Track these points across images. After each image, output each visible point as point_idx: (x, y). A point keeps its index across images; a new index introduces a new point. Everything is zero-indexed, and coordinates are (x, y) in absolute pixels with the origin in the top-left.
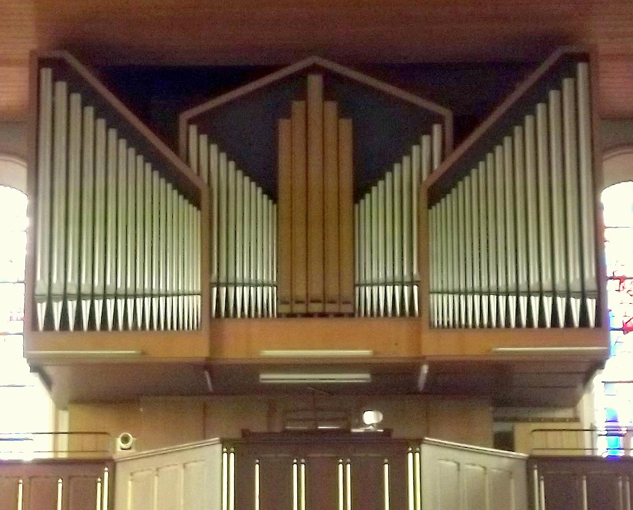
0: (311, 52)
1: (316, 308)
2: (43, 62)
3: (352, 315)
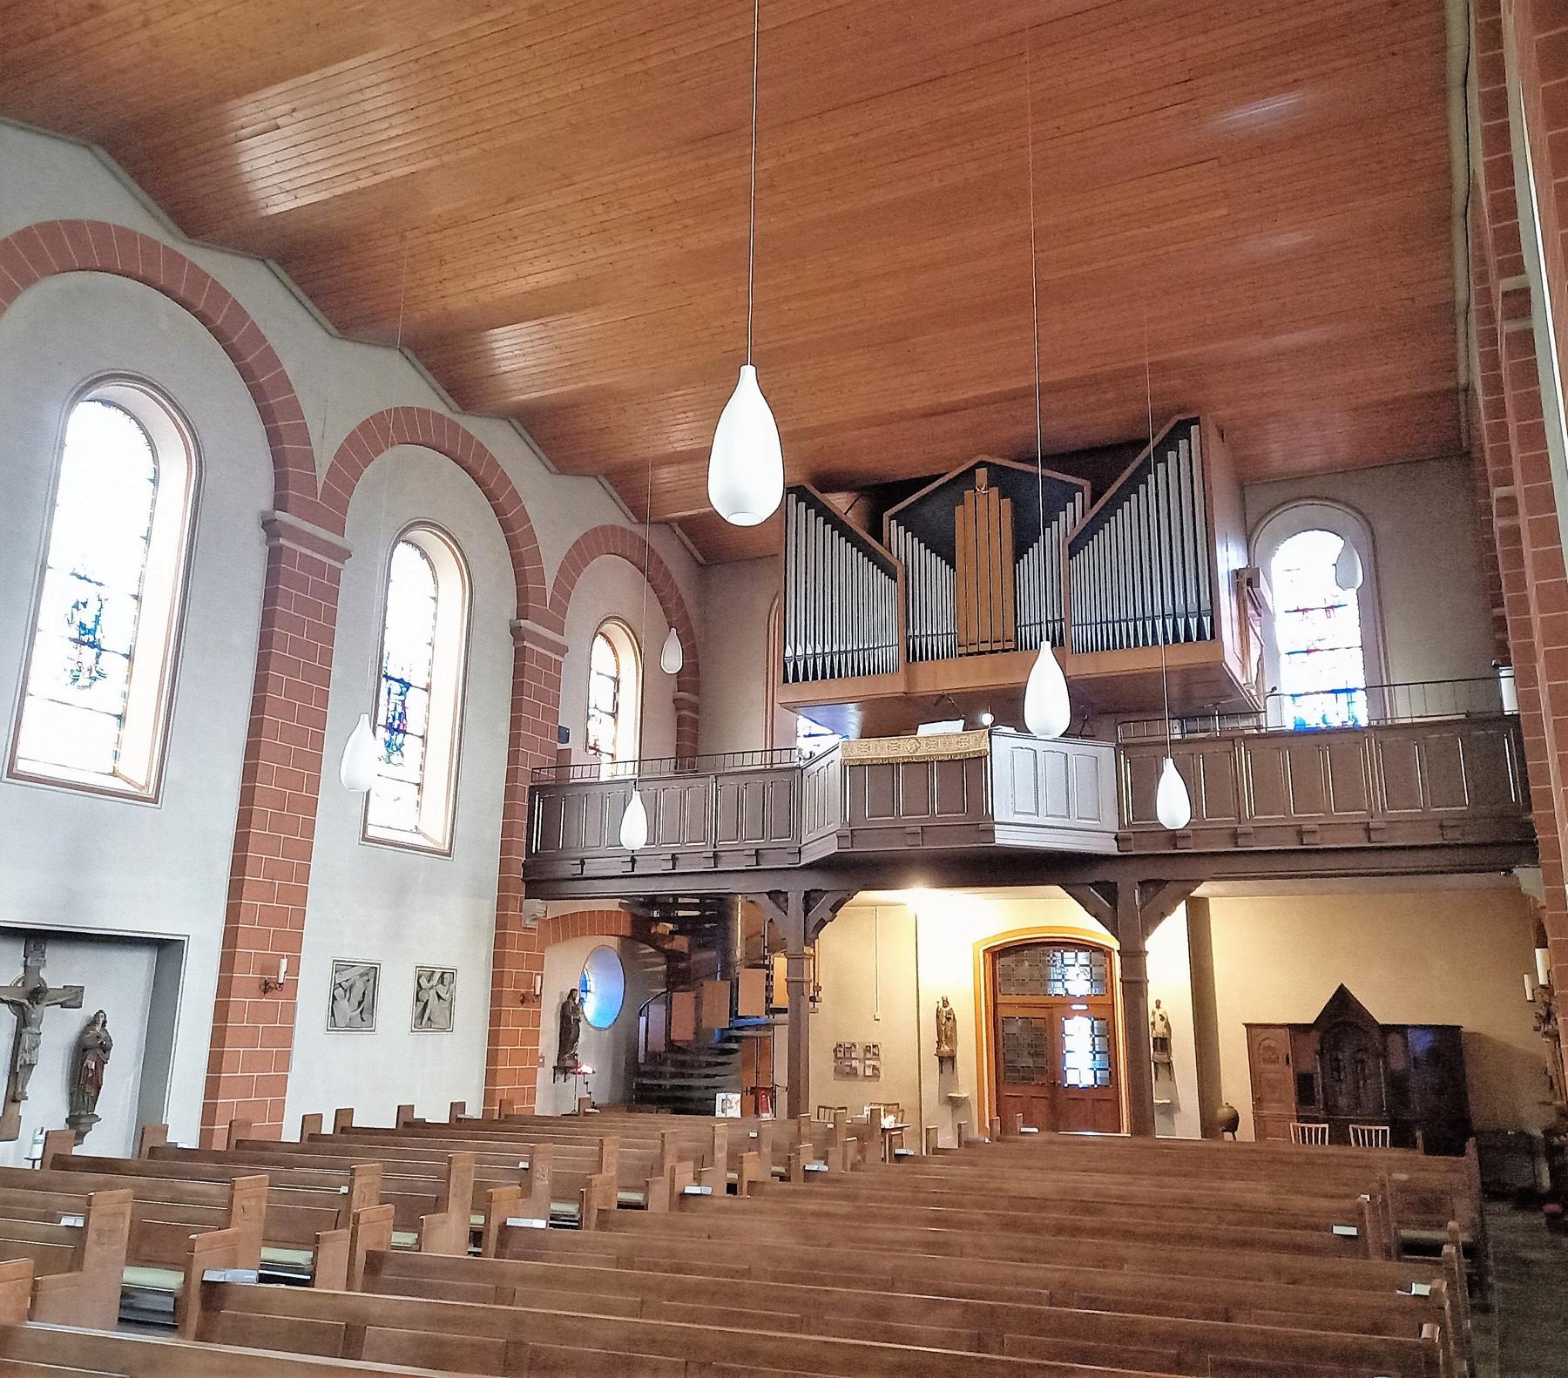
1: (987, 647)
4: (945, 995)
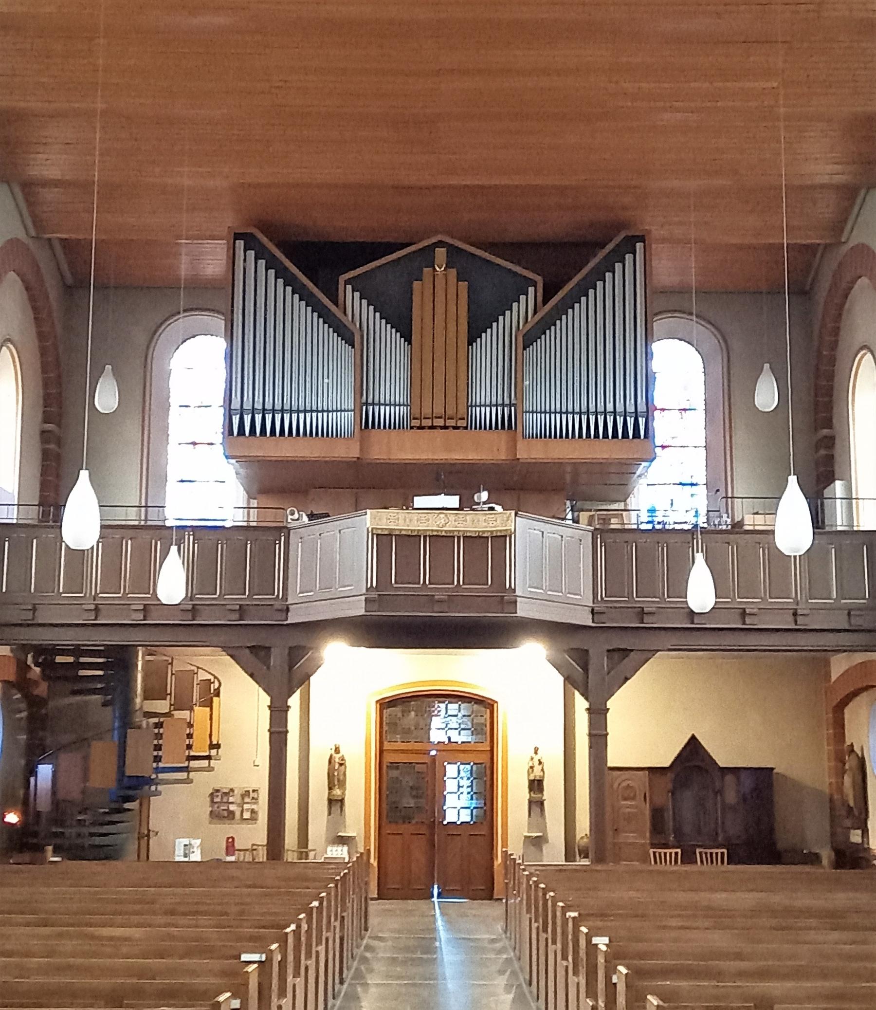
0: (436, 232)
2: (237, 236)
3: (466, 428)
4: (338, 744)
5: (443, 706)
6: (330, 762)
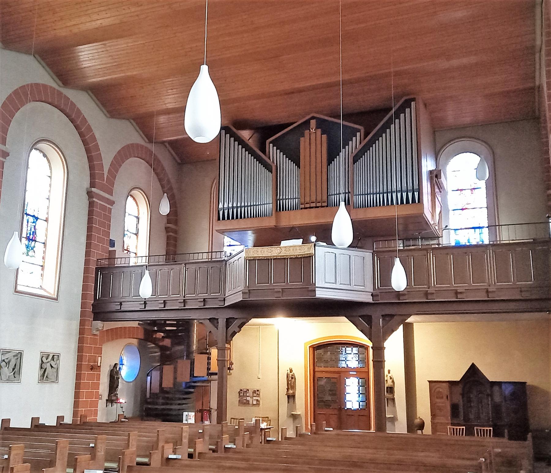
0: (311, 113)
3: (327, 206)
4: (291, 367)
5: (344, 349)
6: (287, 377)
